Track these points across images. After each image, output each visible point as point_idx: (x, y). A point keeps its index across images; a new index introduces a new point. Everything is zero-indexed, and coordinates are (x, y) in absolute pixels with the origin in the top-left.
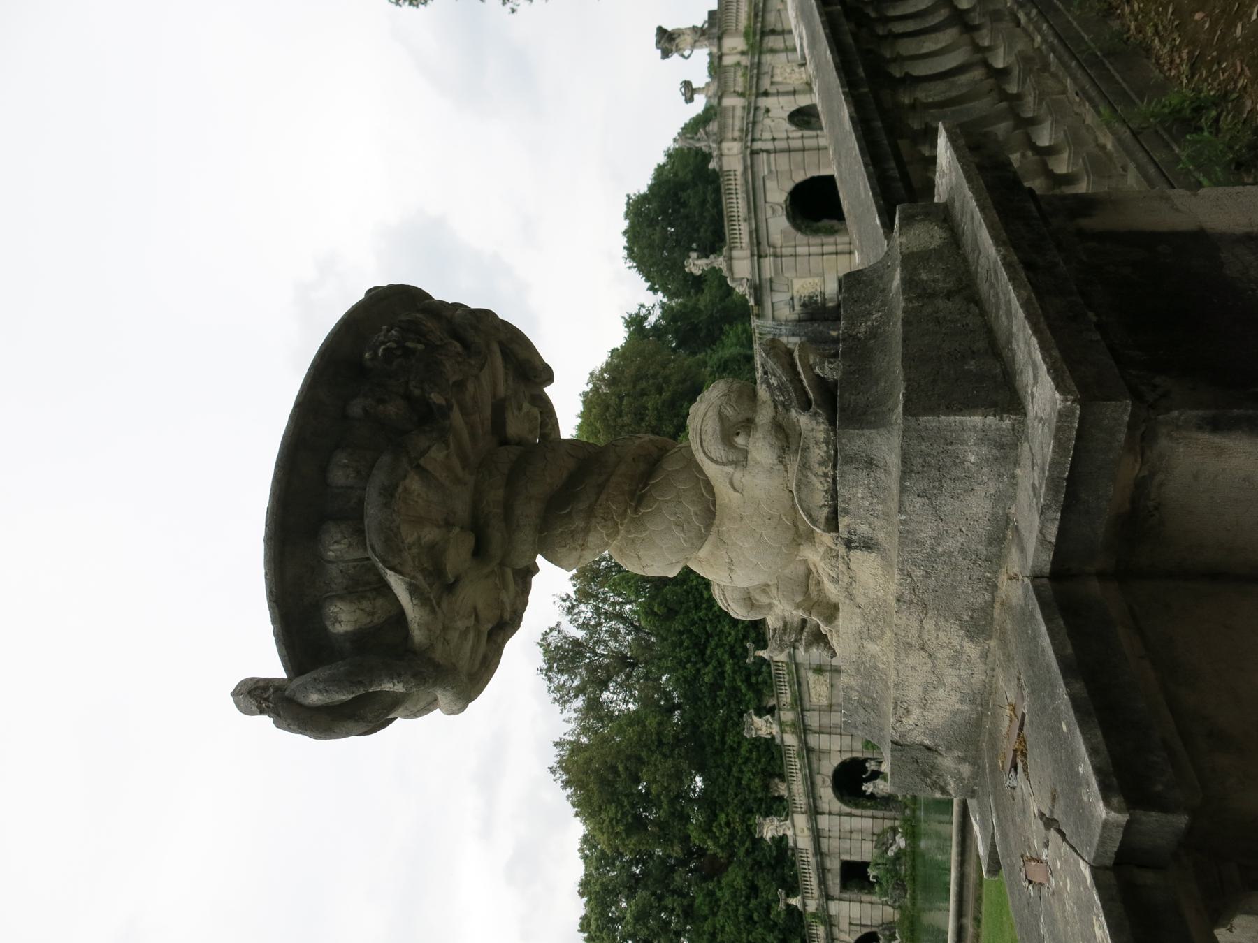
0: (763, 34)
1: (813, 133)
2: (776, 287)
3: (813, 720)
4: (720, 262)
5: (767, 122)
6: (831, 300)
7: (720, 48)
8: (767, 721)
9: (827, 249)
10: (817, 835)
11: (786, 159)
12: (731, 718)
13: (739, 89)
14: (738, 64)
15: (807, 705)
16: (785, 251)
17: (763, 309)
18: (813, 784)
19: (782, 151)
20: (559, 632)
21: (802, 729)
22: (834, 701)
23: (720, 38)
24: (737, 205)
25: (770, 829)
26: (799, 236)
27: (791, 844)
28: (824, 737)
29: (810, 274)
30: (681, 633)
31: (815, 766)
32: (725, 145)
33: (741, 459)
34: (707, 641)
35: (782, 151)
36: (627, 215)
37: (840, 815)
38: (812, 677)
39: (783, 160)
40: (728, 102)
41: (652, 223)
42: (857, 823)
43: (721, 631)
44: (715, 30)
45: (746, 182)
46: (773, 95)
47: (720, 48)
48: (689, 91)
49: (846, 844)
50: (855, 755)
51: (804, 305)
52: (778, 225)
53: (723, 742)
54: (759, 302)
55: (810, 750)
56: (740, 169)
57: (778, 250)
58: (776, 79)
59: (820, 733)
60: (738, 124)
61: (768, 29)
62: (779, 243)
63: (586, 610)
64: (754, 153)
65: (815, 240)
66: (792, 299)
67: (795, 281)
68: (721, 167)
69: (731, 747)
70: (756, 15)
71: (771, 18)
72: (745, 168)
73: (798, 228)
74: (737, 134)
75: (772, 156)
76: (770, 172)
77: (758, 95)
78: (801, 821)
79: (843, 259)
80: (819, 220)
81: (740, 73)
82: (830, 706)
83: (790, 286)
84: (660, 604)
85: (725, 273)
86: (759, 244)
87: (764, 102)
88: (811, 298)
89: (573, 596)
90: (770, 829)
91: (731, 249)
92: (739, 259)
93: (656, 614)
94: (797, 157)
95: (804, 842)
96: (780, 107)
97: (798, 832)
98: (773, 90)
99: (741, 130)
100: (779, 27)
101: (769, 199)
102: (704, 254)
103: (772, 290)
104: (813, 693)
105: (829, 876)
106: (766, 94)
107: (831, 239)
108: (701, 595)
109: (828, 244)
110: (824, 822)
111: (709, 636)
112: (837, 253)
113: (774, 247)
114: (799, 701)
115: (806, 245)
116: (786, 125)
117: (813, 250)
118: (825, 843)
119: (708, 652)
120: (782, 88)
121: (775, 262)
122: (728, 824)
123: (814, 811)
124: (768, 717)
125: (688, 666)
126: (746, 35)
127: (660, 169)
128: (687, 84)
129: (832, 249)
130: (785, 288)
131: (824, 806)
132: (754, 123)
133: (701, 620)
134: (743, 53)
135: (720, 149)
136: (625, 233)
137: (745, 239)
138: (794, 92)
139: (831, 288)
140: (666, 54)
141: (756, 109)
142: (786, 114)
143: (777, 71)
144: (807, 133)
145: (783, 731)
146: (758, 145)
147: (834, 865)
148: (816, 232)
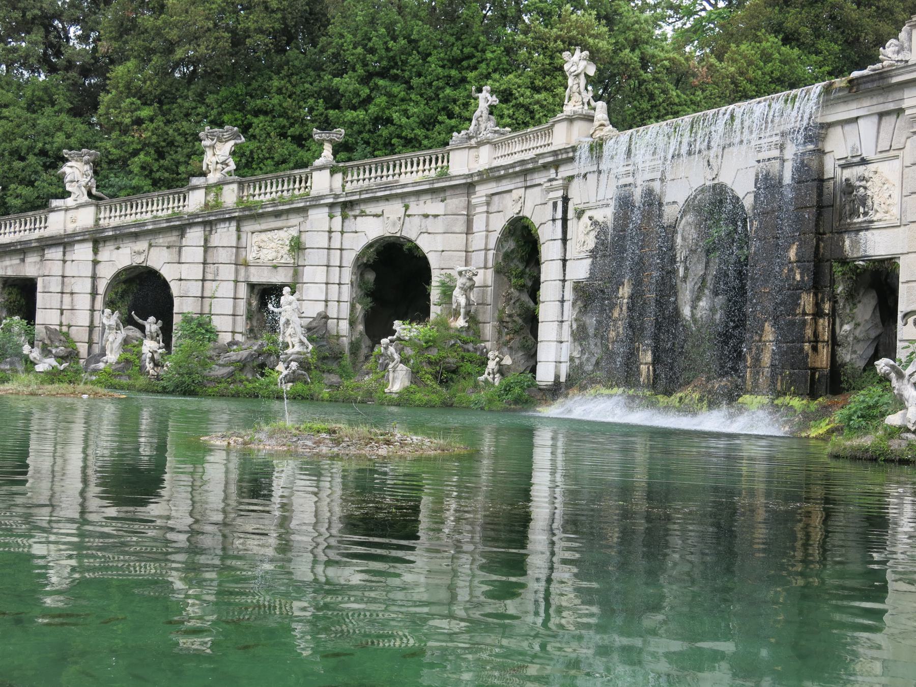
2: (889, 122)
3: (224, 235)
6: (855, 244)
8: (225, 163)
10: (65, 242)
12: (292, 125)
15: (247, 227)
17: (845, 100)
18: (136, 236)
21: (209, 220)
22: (252, 270)
25: (76, 172)
27: (55, 203)
28: (197, 254)
31: (161, 240)
37: (94, 277)
38: (285, 236)
42: (83, 302)
49: (55, 286)
50: (176, 302)
51: (849, 188)
53: (257, 113)
54: (855, 90)
55: (181, 230)
59: (206, 248)
66: (864, 162)
69: (250, 125)
78: (85, 218)
82: (246, 265)
83: (889, 154)
88: (863, 201)
90: (76, 172)
95: (57, 223)
97: (71, 214)
103: (881, 115)
104: (263, 236)
105: (15, 261)
110: (83, 252)
114: (248, 214)
118: (55, 254)
119: (381, 82)
122: (139, 122)
123: (97, 238)
124: (232, 166)
125: (360, 50)
130: (884, 145)
131: (106, 253)
145: (208, 188)
147: (30, 268)
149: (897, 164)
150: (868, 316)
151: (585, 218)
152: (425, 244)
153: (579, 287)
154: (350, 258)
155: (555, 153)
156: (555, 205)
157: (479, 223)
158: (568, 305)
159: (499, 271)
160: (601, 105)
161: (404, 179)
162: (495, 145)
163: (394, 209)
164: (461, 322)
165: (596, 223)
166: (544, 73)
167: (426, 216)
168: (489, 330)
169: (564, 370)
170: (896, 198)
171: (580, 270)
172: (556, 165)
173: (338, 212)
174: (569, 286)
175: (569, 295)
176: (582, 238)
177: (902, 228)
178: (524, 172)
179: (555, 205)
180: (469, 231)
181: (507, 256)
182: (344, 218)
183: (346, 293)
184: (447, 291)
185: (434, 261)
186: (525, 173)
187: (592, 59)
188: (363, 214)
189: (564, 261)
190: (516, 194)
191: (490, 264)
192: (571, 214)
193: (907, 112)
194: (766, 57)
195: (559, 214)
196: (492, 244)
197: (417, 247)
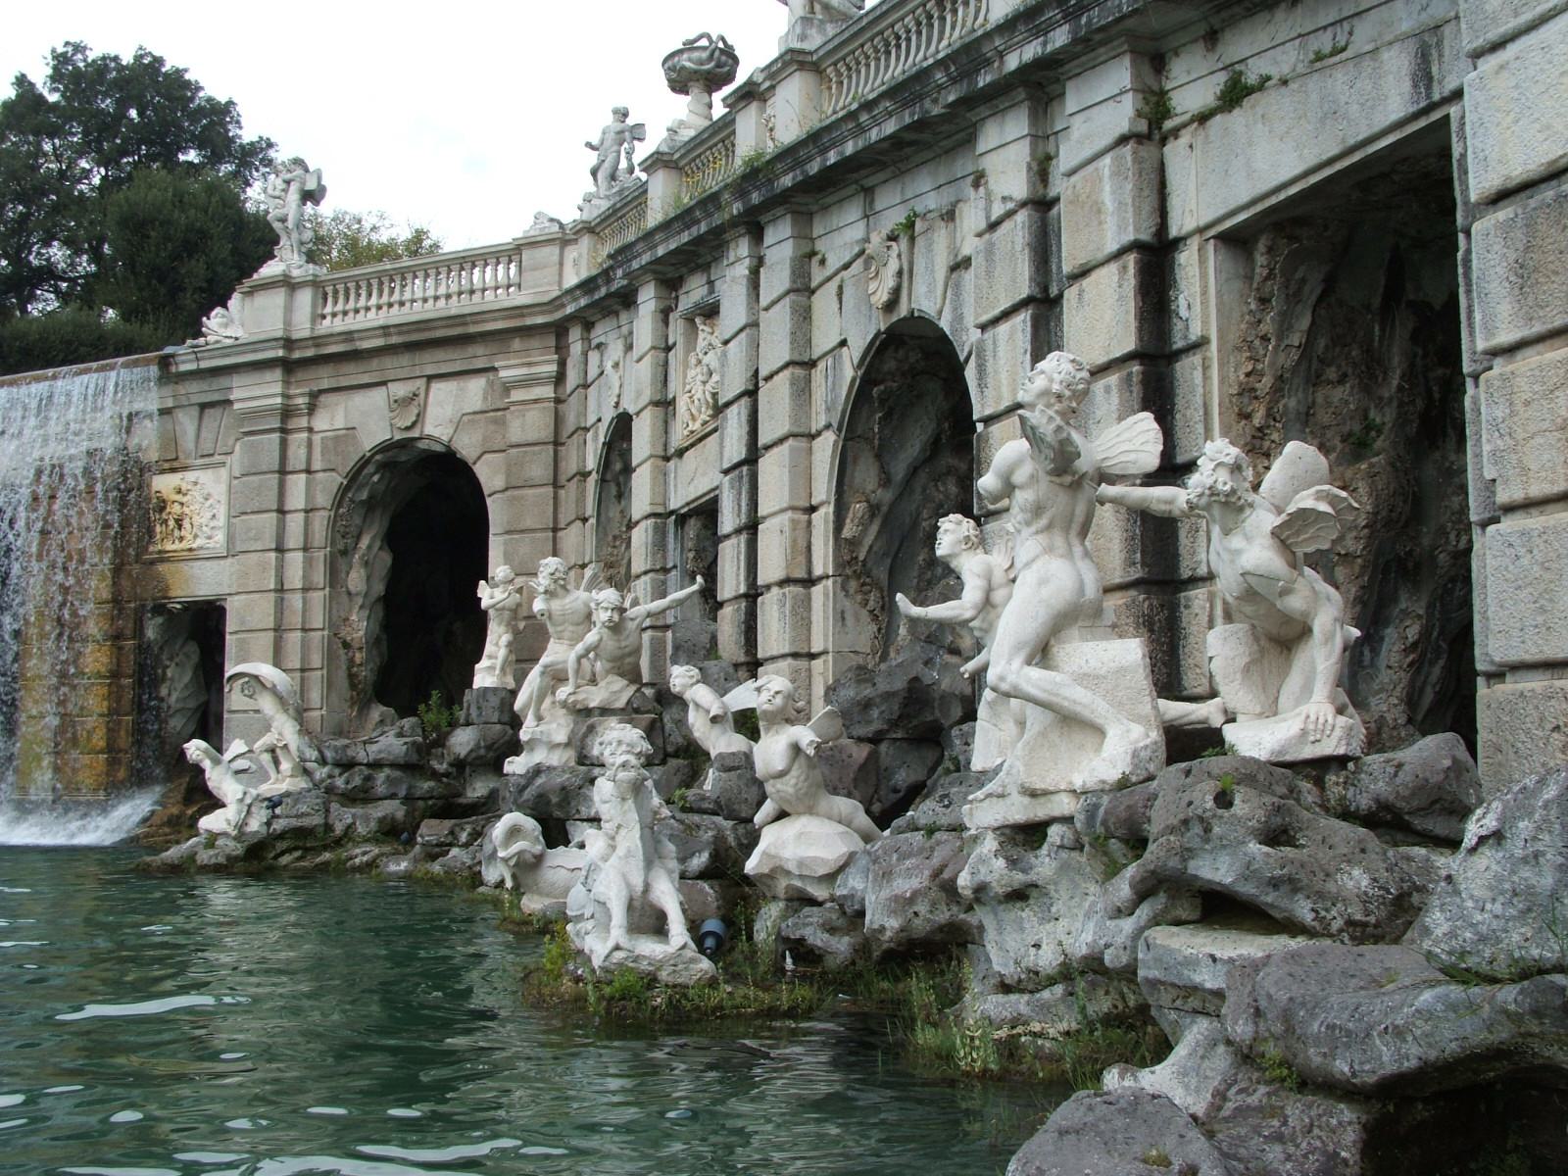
9: (295, 560)
11: (532, 436)
52: (365, 418)
57: (303, 422)
62: (321, 422)
65: (320, 522)
75: (547, 391)
76: (507, 388)
79: (262, 611)
80: (392, 539)
92: (289, 309)
94: (538, 468)
101: (438, 387)
103: (203, 407)
109: (308, 564)
112: (280, 589)
113: (312, 409)
121: (268, 411)
129: (295, 577)
139: (198, 582)
149: (224, 472)
150: (187, 677)
170: (221, 521)
177: (230, 560)
193: (236, 406)
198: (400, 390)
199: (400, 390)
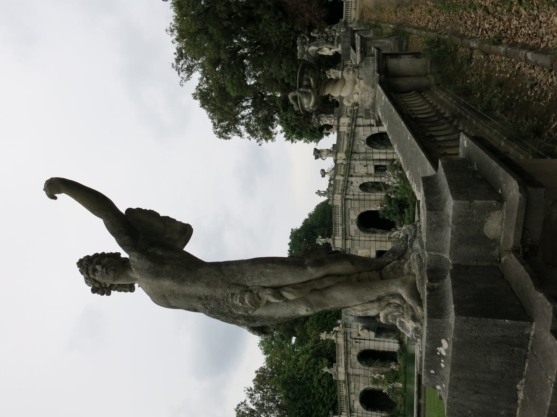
0: (352, 153)
1: (369, 194)
4: (330, 241)
5: (352, 187)
7: (336, 157)
9: (372, 239)
13: (342, 173)
14: (342, 163)
16: (356, 238)
19: (357, 200)
20: (245, 405)
23: (336, 153)
24: (338, 219)
26: (361, 233)
29: (365, 248)
30: (300, 408)
32: (335, 196)
33: (349, 74)
34: (311, 413)
35: (357, 200)
36: (291, 237)
39: (357, 203)
40: (338, 178)
41: (301, 241)
43: (318, 409)
44: (335, 151)
45: (342, 210)
46: (354, 177)
47: (336, 157)
48: (323, 173)
52: (353, 228)
56: (340, 205)
58: (355, 171)
60: (340, 187)
61: (353, 151)
63: (258, 396)
64: (346, 199)
67: (359, 251)
68: (333, 204)
70: (350, 145)
71: (355, 147)
72: (342, 205)
73: (361, 230)
74: (340, 192)
76: (352, 207)
77: (348, 176)
81: (343, 167)
84: (292, 394)
85: (332, 245)
86: (346, 234)
87: (351, 179)
89: (253, 388)
91: (335, 236)
93: (289, 397)
94: (362, 202)
96: (356, 182)
98: (354, 175)
99: (342, 190)
100: (357, 151)
102: (323, 237)
106: (352, 176)
107: (374, 235)
108: (311, 391)
111: (313, 411)
115: (364, 237)
116: (359, 190)
117: (367, 239)
120: (357, 174)
126: (346, 153)
127: (306, 220)
128: (323, 171)
129: (374, 239)
132: (347, 187)
133: (310, 403)
134: (344, 160)
135: (333, 197)
136: (289, 244)
137: (341, 232)
138: (362, 176)
139: (373, 255)
140: (317, 158)
141: (348, 181)
142: (358, 185)
143: (356, 168)
144: (366, 193)
146: (348, 197)
148: (368, 232)
151: (360, 332)
152: (362, 389)
153: (376, 336)
154: (365, 411)
155: (344, 340)
156: (356, 342)
157: (357, 372)
158: (381, 339)
159: (370, 366)
160: (334, 329)
161: (345, 394)
162: (338, 366)
163: (353, 397)
164: (383, 376)
165: (362, 329)
166: (314, 371)
167: (355, 388)
168: (385, 370)
169: (396, 341)
171: (372, 334)
172: (347, 341)
173: (352, 414)
174: (376, 339)
175: (378, 339)
176: (364, 335)
178: (347, 353)
179: (356, 342)
180: (358, 375)
181: (366, 364)
182: (354, 412)
183: (374, 413)
184: (375, 381)
185: (366, 387)
186: (347, 353)
187: (323, 332)
188: (353, 406)
189: (370, 340)
190: (352, 358)
191: (368, 368)
192: (359, 338)
194: (312, 324)
195: (358, 341)
196: (363, 367)
197: (362, 391)
198: (350, 223)
199: (350, 223)
